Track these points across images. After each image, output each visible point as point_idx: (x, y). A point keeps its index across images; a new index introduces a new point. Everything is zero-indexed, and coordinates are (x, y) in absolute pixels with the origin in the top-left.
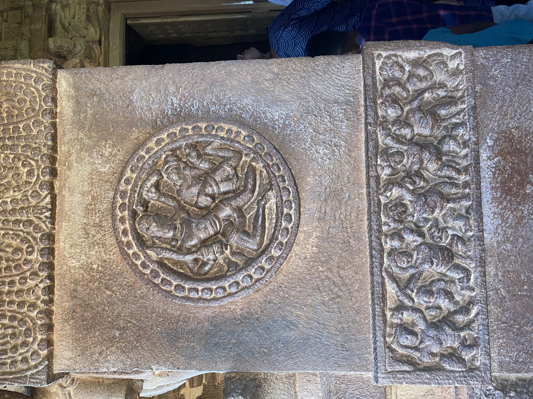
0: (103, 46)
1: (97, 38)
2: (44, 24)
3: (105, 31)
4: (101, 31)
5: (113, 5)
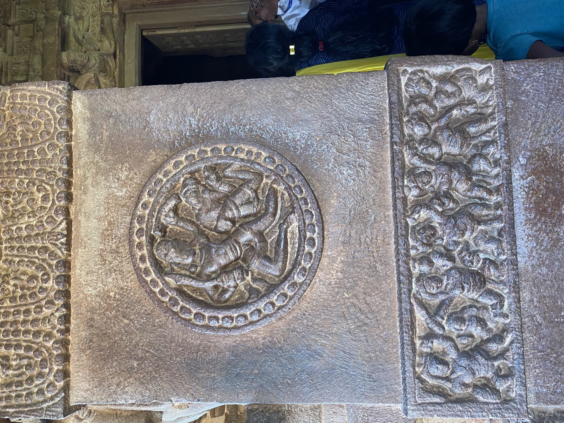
1: (112, 51)
2: (57, 38)
3: (120, 44)
4: (116, 44)
5: (128, 17)
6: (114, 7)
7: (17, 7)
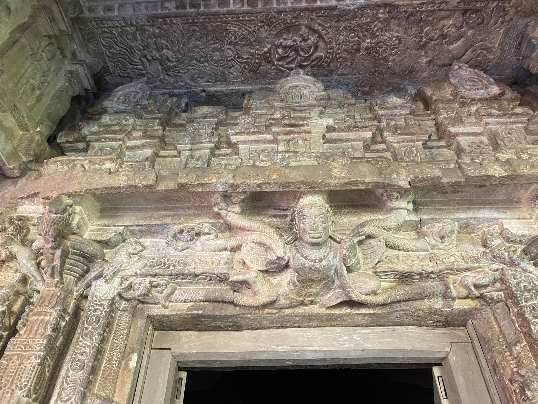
0: (349, 311)
2: (343, 181)
3: (385, 314)
4: (383, 305)
5: (460, 332)
6: (469, 301)
7: (420, 143)
